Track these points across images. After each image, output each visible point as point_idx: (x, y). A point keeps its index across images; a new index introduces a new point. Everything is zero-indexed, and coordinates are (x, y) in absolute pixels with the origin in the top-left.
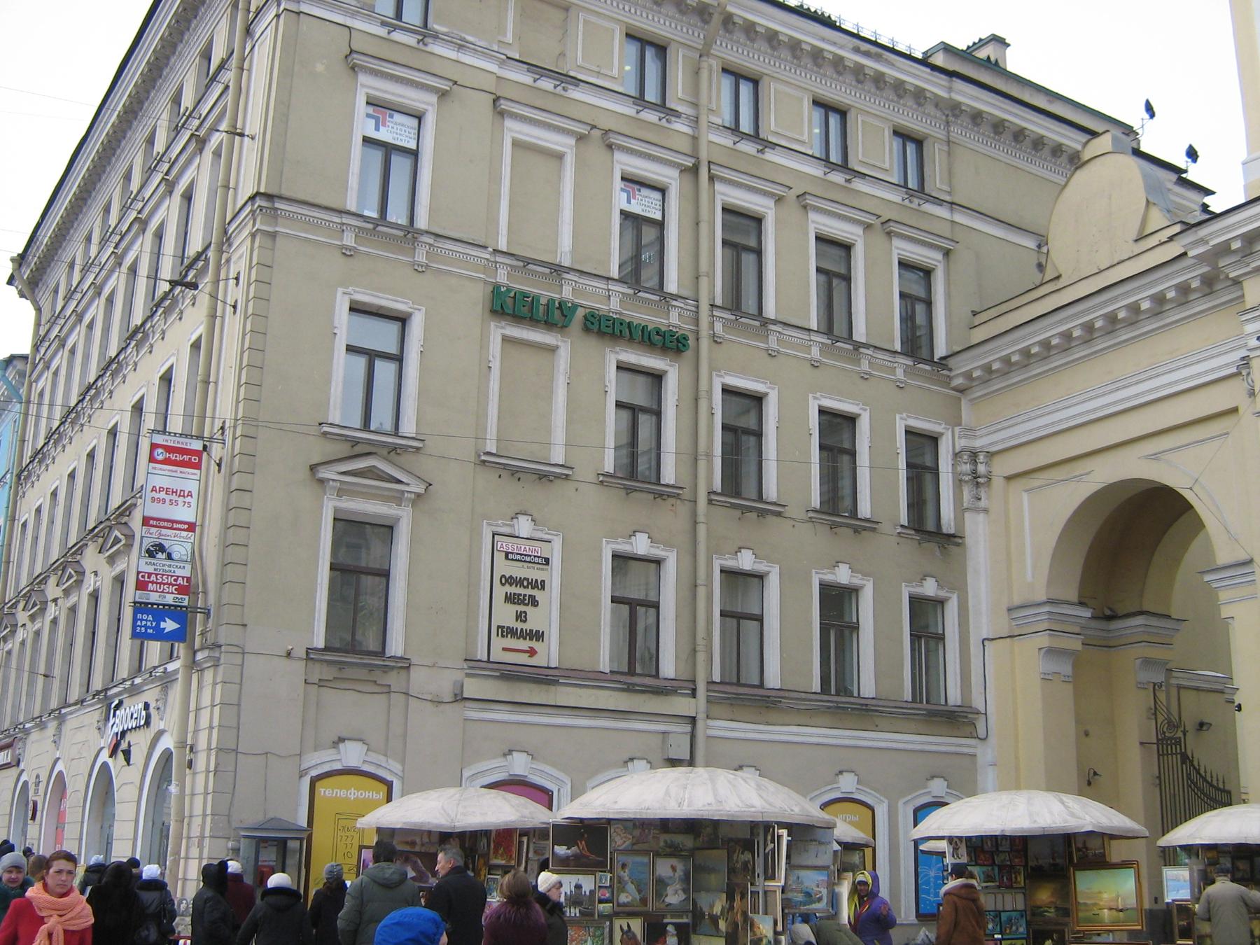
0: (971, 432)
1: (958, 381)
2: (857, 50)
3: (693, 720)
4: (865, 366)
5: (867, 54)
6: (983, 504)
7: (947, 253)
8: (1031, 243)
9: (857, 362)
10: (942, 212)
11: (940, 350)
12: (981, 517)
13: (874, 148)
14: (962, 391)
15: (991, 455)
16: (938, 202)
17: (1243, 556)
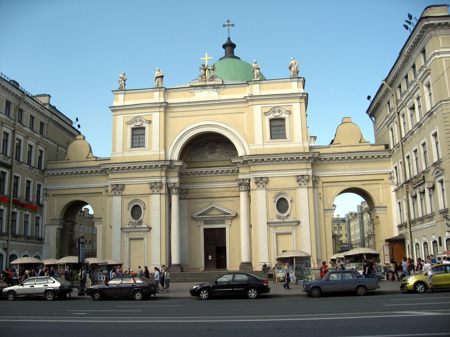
0: (46, 185)
1: (46, 175)
2: (40, 108)
3: (8, 241)
4: (33, 171)
5: (42, 109)
6: (47, 199)
7: (46, 148)
8: (56, 146)
9: (32, 170)
10: (45, 140)
11: (42, 168)
12: (46, 202)
13: (37, 127)
14: (45, 176)
15: (50, 190)
16: (45, 138)
17: (100, 217)
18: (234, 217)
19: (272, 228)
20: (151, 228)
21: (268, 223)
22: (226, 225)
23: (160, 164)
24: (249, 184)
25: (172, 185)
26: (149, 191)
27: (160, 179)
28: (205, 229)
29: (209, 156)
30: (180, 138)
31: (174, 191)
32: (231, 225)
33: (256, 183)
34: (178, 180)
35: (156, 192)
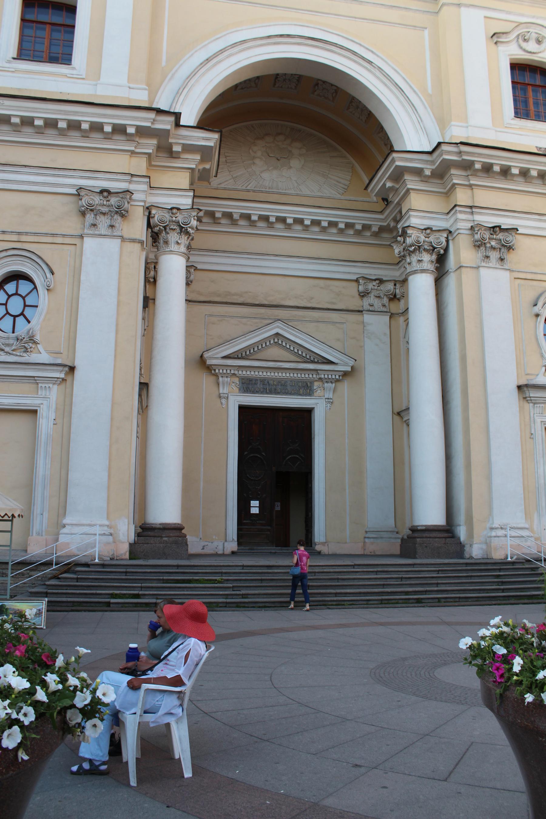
18: (345, 374)
19: (528, 407)
20: (72, 369)
21: (519, 387)
22: (318, 404)
23: (132, 121)
24: (446, 250)
25: (167, 217)
26: (72, 225)
27: (123, 186)
28: (243, 410)
29: (266, 175)
30: (208, 60)
31: (173, 237)
32: (330, 401)
33: (479, 245)
34: (189, 201)
35: (103, 232)
